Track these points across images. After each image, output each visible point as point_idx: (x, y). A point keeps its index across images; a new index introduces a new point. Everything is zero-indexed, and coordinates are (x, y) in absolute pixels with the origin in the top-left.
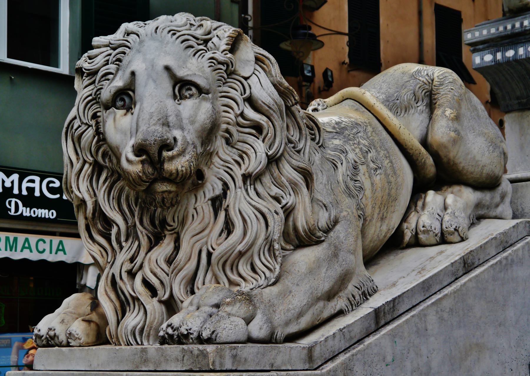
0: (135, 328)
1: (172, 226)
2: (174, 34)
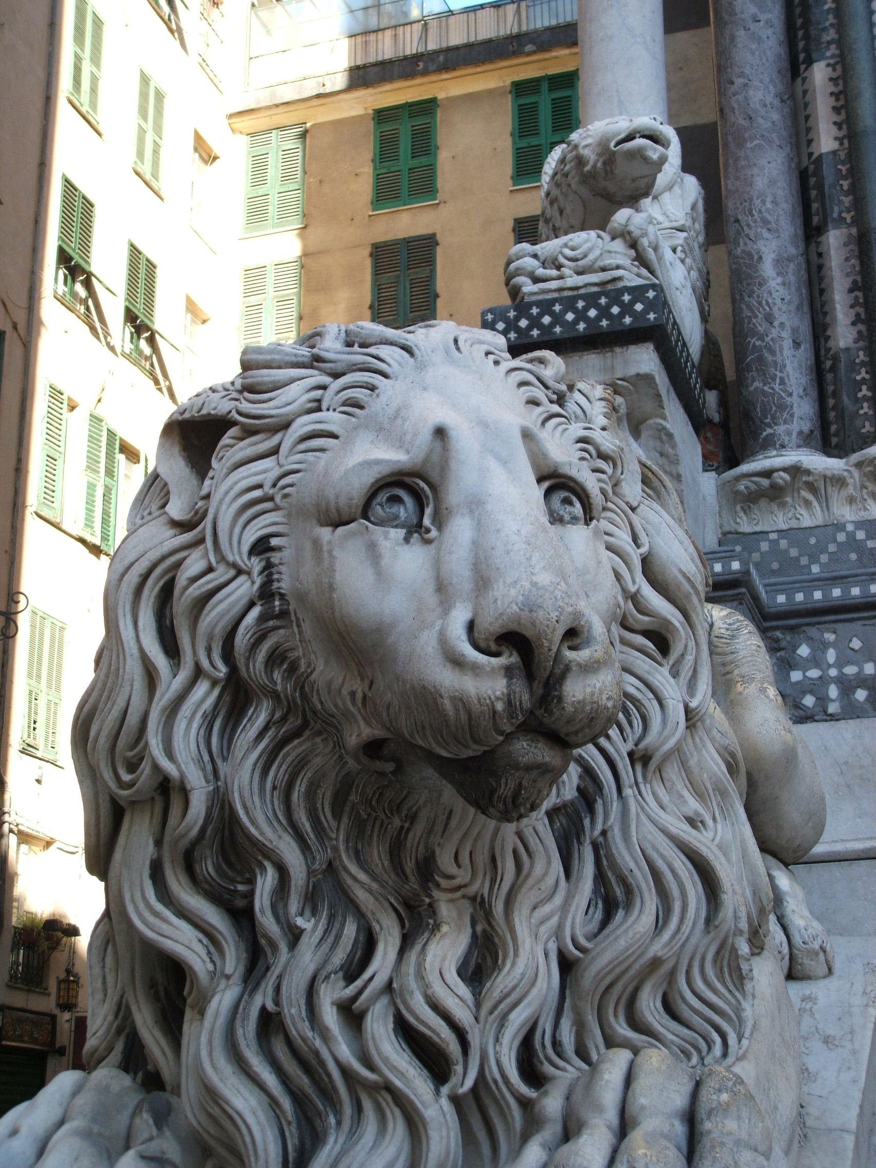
1: (451, 877)
2: (496, 363)
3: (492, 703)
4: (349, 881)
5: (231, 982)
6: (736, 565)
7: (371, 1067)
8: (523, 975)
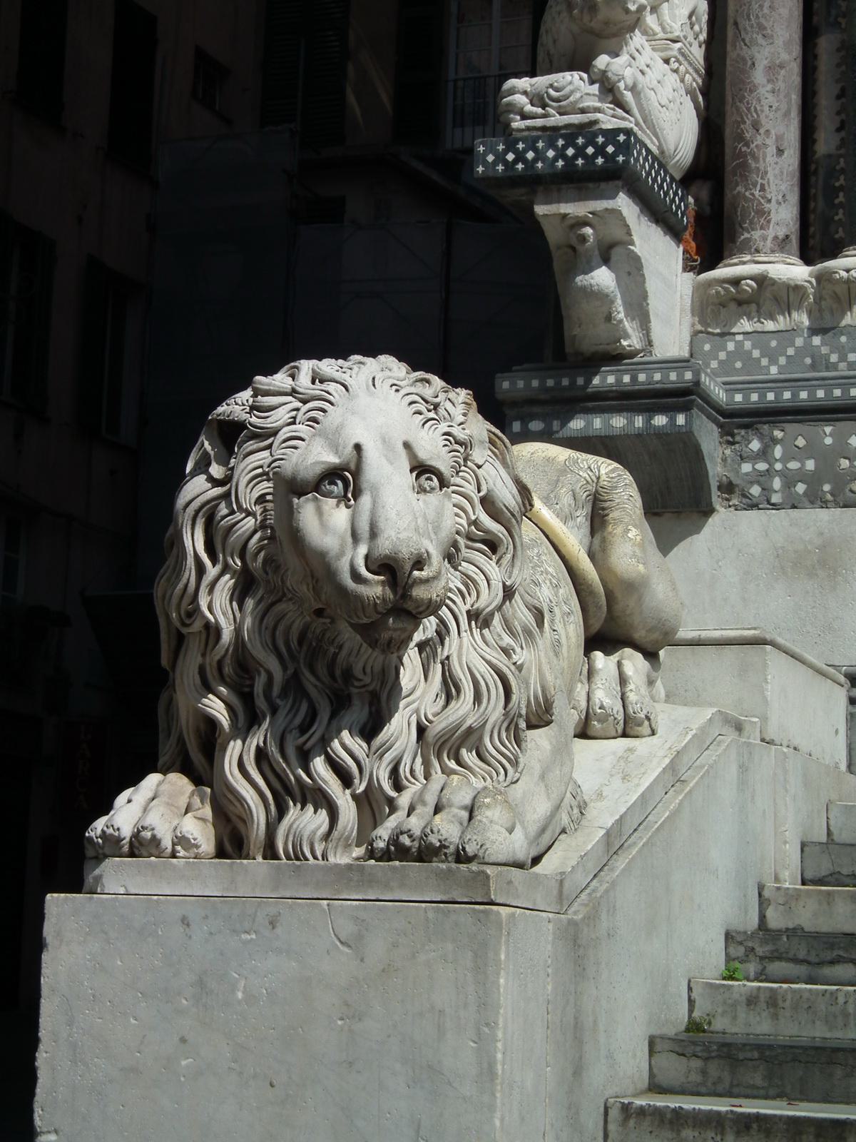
0: (314, 832)
1: (360, 680)
6: (688, 376)
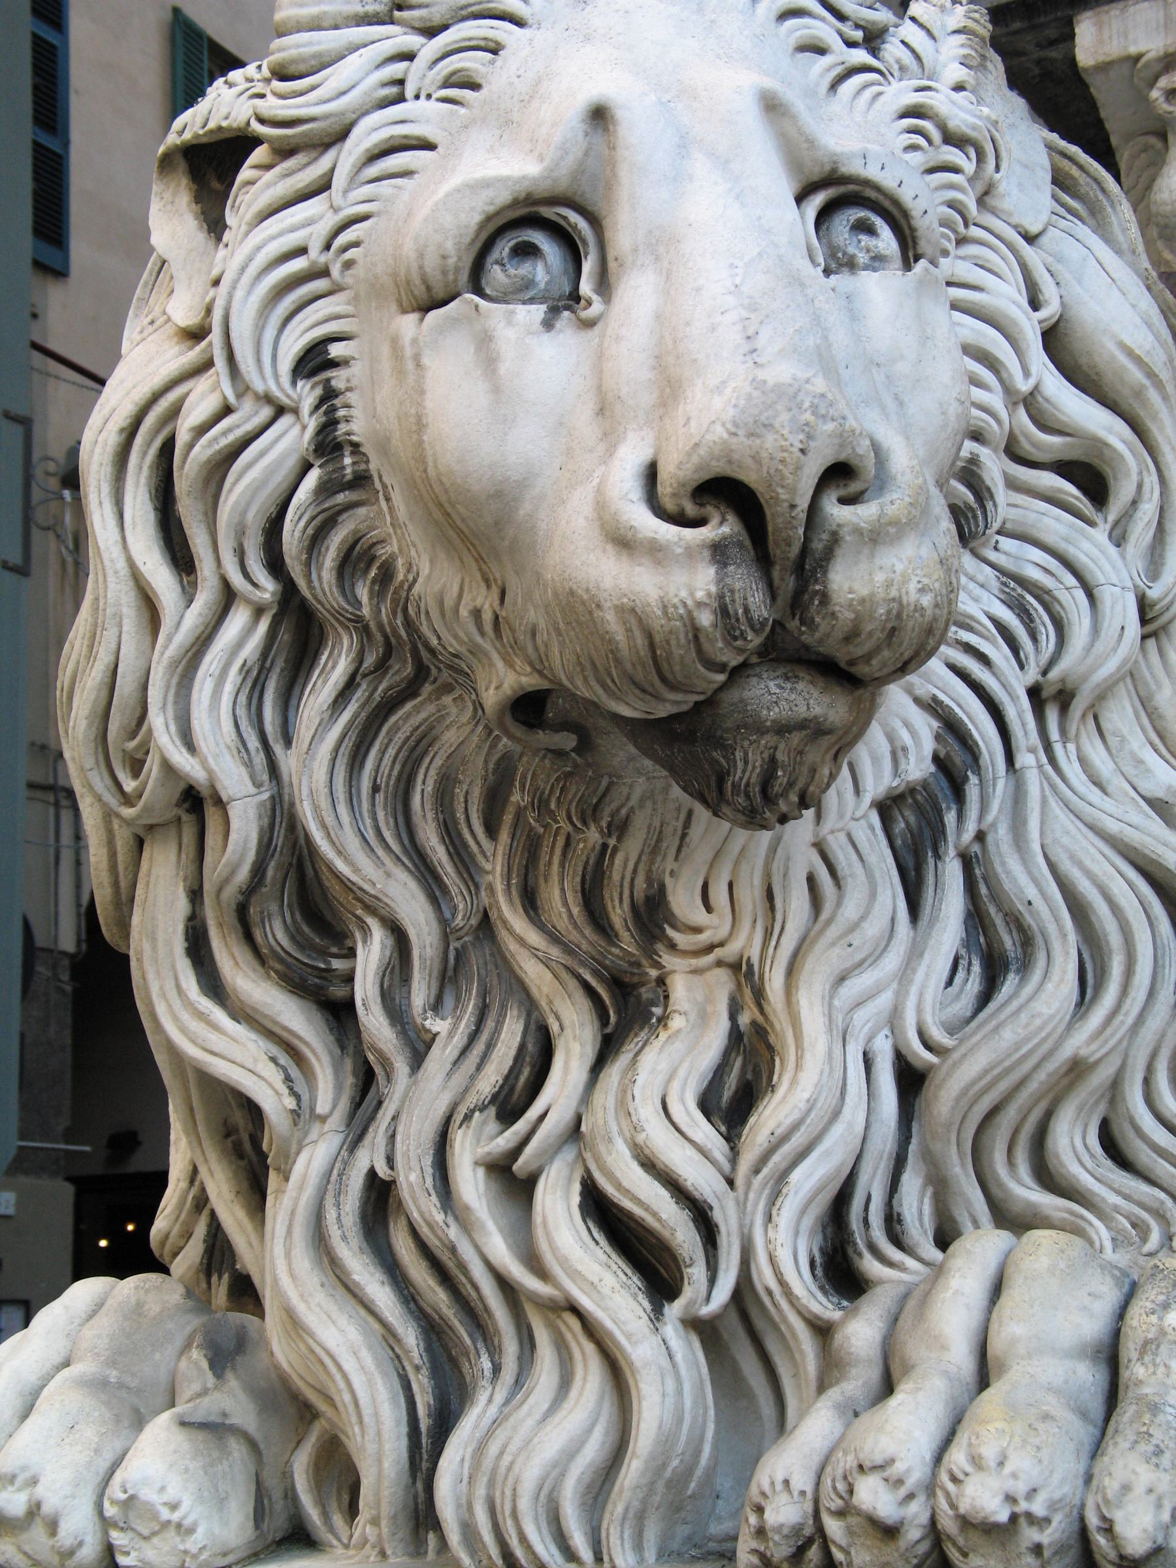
1: (697, 930)
3: (690, 612)
4: (512, 946)
5: (327, 1127)
7: (541, 1272)
8: (811, 1104)
